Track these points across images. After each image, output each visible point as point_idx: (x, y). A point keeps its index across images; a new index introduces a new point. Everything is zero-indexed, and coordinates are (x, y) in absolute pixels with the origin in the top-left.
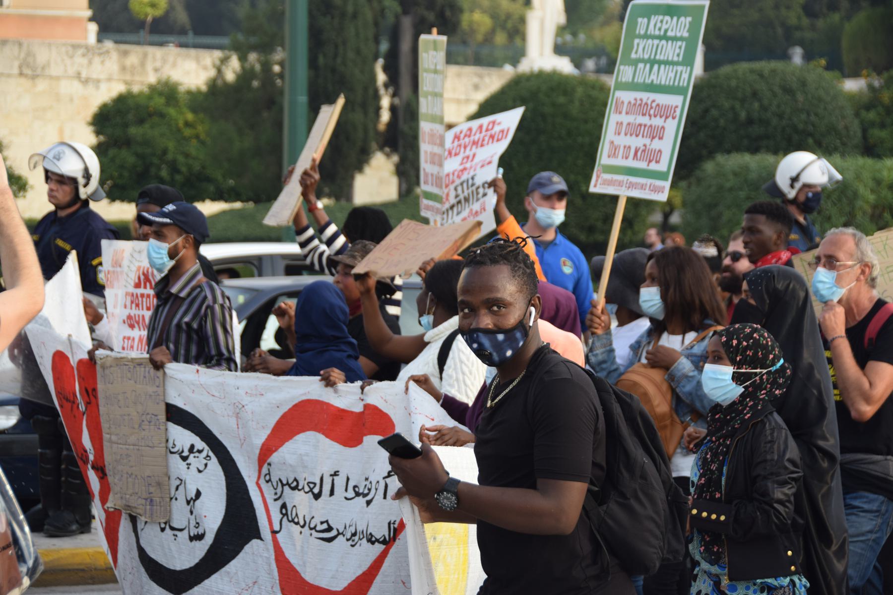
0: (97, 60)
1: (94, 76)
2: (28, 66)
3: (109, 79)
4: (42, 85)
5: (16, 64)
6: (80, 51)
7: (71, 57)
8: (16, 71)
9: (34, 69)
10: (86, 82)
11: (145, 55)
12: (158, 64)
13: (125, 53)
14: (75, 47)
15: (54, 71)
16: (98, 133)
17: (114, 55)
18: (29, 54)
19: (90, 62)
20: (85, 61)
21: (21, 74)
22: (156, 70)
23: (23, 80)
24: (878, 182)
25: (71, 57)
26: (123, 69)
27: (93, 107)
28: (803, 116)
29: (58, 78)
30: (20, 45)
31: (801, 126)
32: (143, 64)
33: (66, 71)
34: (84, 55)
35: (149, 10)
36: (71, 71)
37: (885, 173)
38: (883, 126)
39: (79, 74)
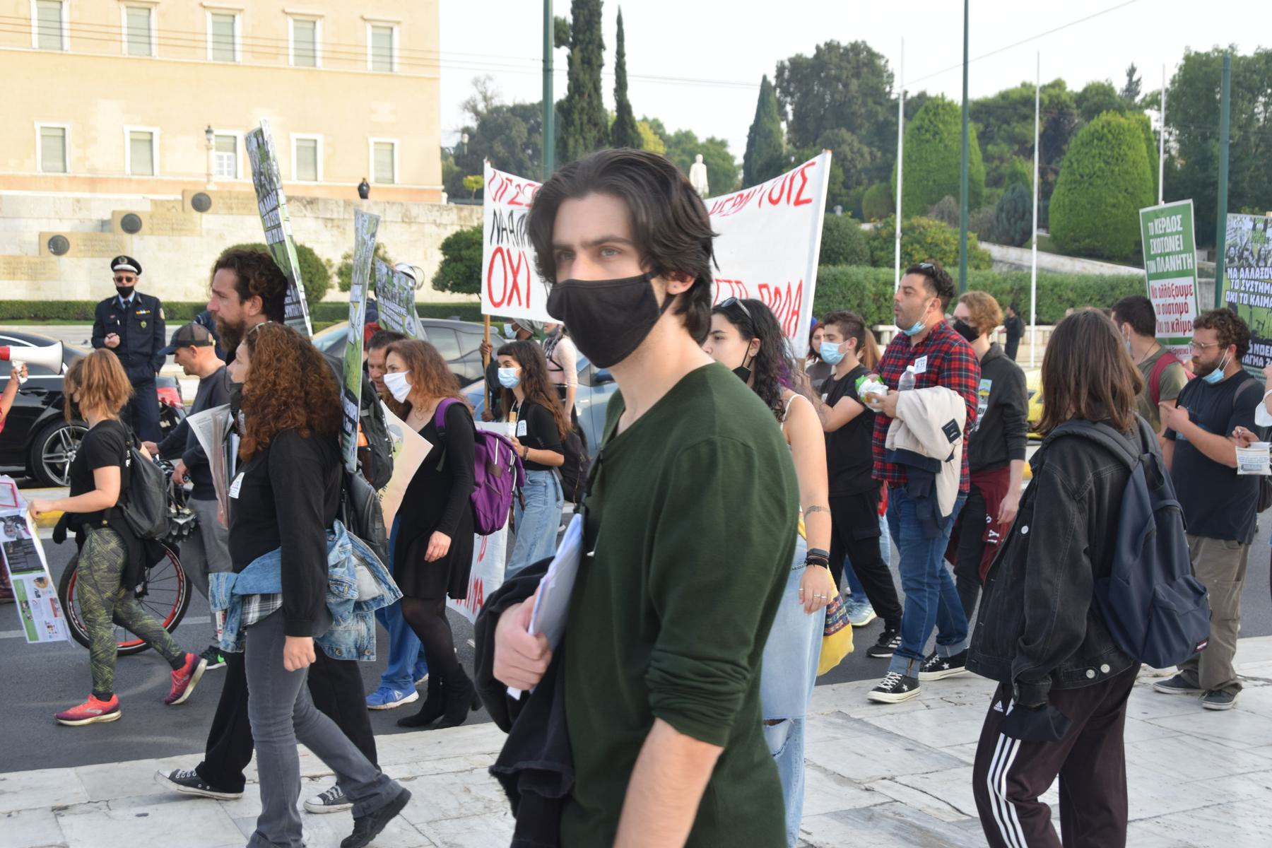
0: (445, 213)
2: (407, 217)
3: (452, 224)
4: (414, 227)
5: (400, 215)
6: (436, 209)
8: (400, 220)
9: (410, 219)
10: (439, 225)
11: (472, 210)
12: (479, 216)
13: (461, 210)
14: (433, 206)
15: (422, 219)
16: (444, 254)
17: (455, 211)
18: (408, 210)
19: (441, 215)
20: (438, 214)
21: (403, 221)
22: (478, 219)
23: (404, 225)
24: (877, 280)
25: (431, 212)
26: (460, 218)
27: (442, 240)
28: (838, 244)
29: (423, 223)
30: (402, 204)
31: (836, 249)
32: (471, 216)
34: (438, 211)
35: (474, 185)
36: (431, 219)
37: (881, 276)
38: (882, 249)
39: (435, 221)
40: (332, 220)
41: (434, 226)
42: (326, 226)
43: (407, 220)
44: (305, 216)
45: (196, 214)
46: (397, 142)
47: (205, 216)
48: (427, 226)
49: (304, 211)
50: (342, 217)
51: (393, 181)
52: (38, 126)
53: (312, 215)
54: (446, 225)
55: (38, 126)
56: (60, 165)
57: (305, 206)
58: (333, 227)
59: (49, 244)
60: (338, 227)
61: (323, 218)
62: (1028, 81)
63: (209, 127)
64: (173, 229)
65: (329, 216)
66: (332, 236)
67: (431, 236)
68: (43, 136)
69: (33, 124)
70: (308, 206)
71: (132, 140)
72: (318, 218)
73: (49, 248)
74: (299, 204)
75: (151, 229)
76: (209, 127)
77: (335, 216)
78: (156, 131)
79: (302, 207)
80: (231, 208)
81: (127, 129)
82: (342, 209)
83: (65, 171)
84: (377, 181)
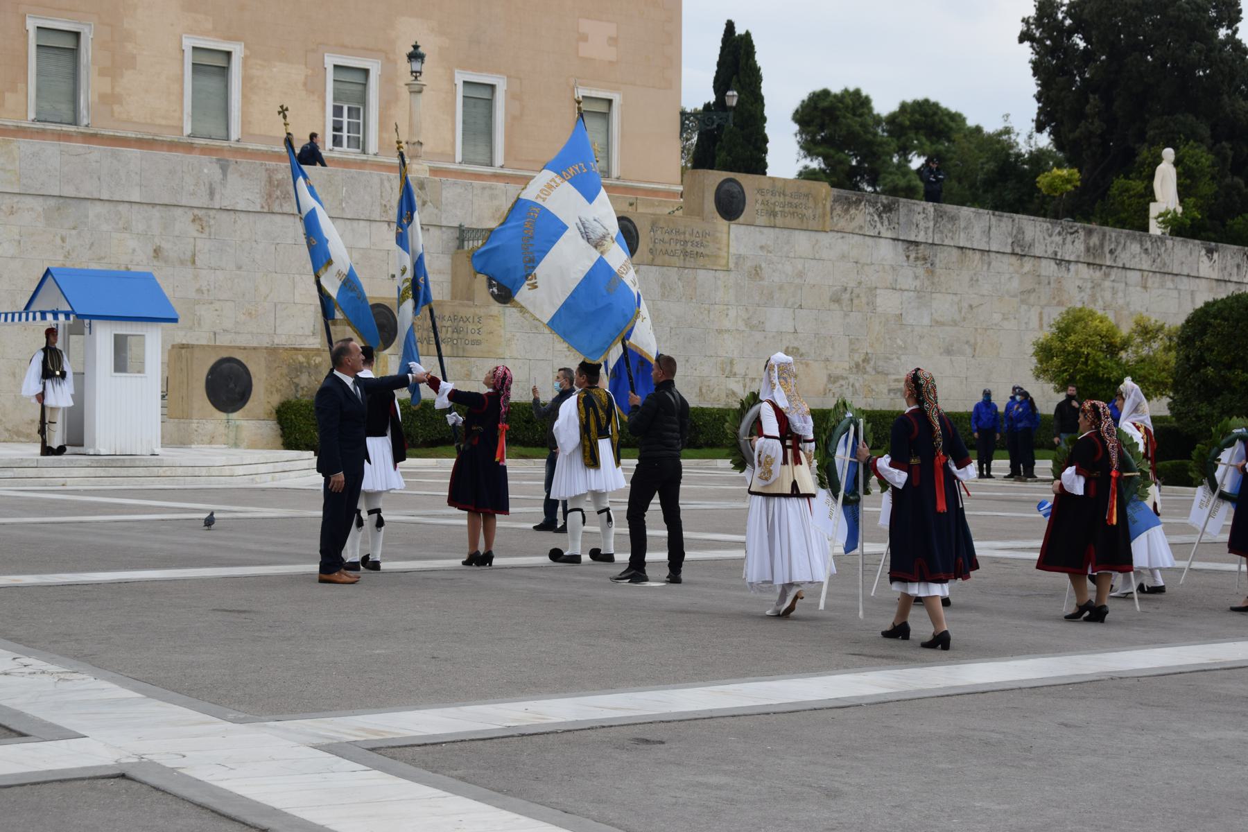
0: (1069, 238)
1: (1067, 258)
3: (1077, 262)
4: (1028, 265)
5: (1010, 241)
7: (1050, 236)
10: (1060, 262)
12: (1113, 246)
13: (1089, 233)
17: (1082, 233)
19: (1064, 240)
20: (1058, 239)
21: (1013, 254)
23: (1013, 259)
25: (1050, 236)
26: (1088, 250)
29: (1039, 257)
32: (1102, 245)
33: (1046, 252)
34: (1059, 234)
39: (1056, 253)
40: (917, 244)
41: (1053, 263)
42: (908, 257)
43: (1018, 250)
44: (879, 236)
45: (722, 223)
46: (617, 98)
47: (734, 227)
48: (1044, 262)
49: (879, 225)
50: (930, 241)
52: (31, 25)
53: (889, 234)
54: (1069, 262)
55: (31, 25)
56: (65, 109)
57: (880, 216)
58: (917, 259)
60: (925, 259)
63: (416, 47)
64: (685, 254)
65: (913, 238)
66: (916, 277)
67: (1049, 283)
68: (38, 46)
69: (24, 21)
70: (884, 215)
71: (196, 67)
72: (898, 240)
74: (871, 210)
75: (651, 251)
76: (416, 47)
77: (921, 238)
78: (238, 50)
79: (876, 218)
81: (188, 43)
82: (931, 224)
83: (75, 122)
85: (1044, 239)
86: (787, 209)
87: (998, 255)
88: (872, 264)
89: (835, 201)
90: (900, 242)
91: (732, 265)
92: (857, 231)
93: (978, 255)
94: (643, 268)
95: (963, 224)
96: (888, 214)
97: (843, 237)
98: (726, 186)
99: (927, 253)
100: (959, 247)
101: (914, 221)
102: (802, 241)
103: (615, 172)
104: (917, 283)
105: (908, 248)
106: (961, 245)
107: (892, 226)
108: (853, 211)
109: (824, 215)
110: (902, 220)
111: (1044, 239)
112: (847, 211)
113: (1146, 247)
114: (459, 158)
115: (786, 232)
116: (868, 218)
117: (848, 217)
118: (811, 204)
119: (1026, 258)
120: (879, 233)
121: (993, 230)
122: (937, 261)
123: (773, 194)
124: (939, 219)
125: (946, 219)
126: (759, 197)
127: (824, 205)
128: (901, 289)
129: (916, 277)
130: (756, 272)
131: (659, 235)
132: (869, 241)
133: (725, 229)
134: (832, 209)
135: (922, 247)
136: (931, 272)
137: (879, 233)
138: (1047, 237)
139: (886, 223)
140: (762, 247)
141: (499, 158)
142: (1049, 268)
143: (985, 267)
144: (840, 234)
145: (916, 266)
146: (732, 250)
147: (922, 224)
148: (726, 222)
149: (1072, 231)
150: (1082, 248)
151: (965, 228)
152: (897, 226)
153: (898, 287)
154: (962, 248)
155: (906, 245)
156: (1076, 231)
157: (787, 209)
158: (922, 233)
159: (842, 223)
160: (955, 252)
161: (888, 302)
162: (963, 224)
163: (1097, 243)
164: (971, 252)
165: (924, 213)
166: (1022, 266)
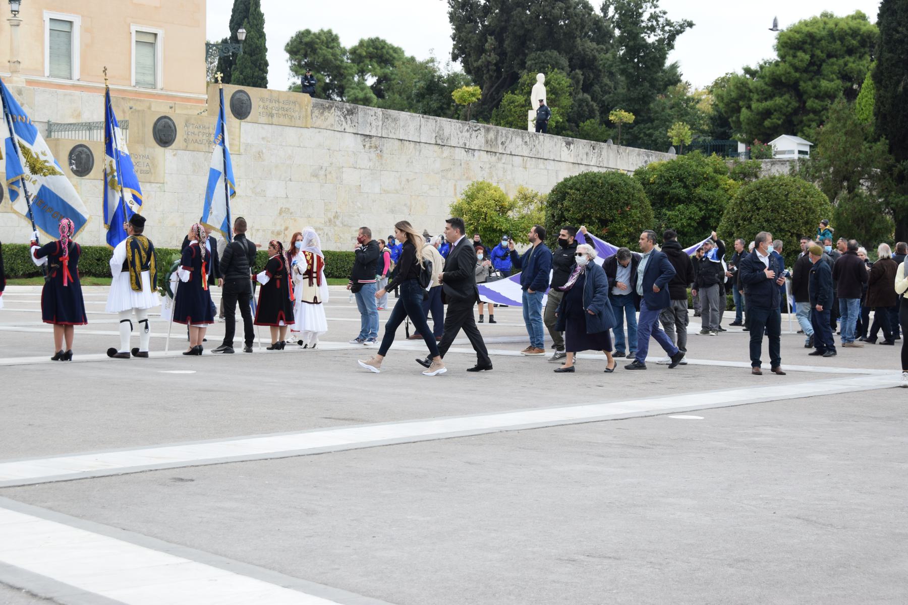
0: (474, 134)
1: (473, 148)
4: (447, 151)
5: (434, 135)
7: (461, 132)
10: (469, 151)
12: (503, 140)
13: (488, 130)
17: (483, 130)
18: (441, 127)
20: (467, 135)
23: (436, 147)
25: (461, 132)
26: (487, 142)
32: (496, 139)
33: (459, 143)
36: (461, 144)
40: (370, 137)
41: (463, 150)
42: (364, 146)
43: (439, 142)
44: (344, 131)
46: (161, 33)
47: (244, 124)
49: (344, 123)
51: (154, 86)
53: (352, 130)
54: (474, 150)
57: (345, 117)
58: (371, 147)
59: (70, 158)
60: (376, 147)
61: (361, 134)
62: (829, 11)
65: (368, 133)
66: (370, 160)
67: (461, 164)
70: (348, 117)
72: (358, 134)
73: (71, 164)
74: (339, 113)
75: (185, 140)
79: (342, 119)
80: (271, 115)
82: (380, 123)
84: (137, 83)
85: (457, 134)
86: (280, 112)
87: (425, 145)
88: (340, 150)
89: (314, 107)
90: (359, 136)
91: (242, 151)
92: (329, 127)
93: (412, 144)
94: (180, 152)
95: (402, 124)
96: (351, 116)
97: (319, 132)
98: (238, 96)
99: (377, 143)
100: (399, 139)
101: (369, 121)
102: (291, 134)
103: (160, 85)
104: (371, 164)
105: (364, 140)
106: (401, 138)
107: (353, 125)
108: (326, 114)
109: (306, 116)
110: (360, 120)
111: (457, 134)
112: (322, 113)
113: (525, 140)
114: (47, 73)
115: (280, 128)
116: (337, 119)
117: (323, 118)
118: (297, 108)
119: (445, 147)
120: (345, 129)
121: (422, 127)
122: (384, 149)
123: (271, 101)
124: (386, 120)
125: (390, 120)
126: (261, 104)
127: (306, 109)
128: (359, 168)
129: (370, 160)
130: (259, 155)
131: (191, 129)
132: (338, 135)
133: (238, 125)
134: (312, 113)
135: (374, 139)
136: (380, 156)
137: (345, 129)
138: (459, 133)
139: (349, 122)
140: (263, 138)
141: (76, 74)
142: (460, 154)
143: (417, 153)
144: (317, 130)
145: (370, 152)
146: (242, 140)
147: (374, 123)
148: (238, 121)
149: (476, 129)
150: (483, 140)
151: (404, 126)
152: (356, 125)
153: (358, 167)
154: (401, 140)
155: (364, 138)
156: (479, 129)
157: (280, 112)
158: (374, 129)
159: (319, 122)
160: (397, 143)
161: (351, 177)
162: (402, 124)
163: (493, 137)
164: (408, 142)
165: (375, 115)
166: (442, 152)
